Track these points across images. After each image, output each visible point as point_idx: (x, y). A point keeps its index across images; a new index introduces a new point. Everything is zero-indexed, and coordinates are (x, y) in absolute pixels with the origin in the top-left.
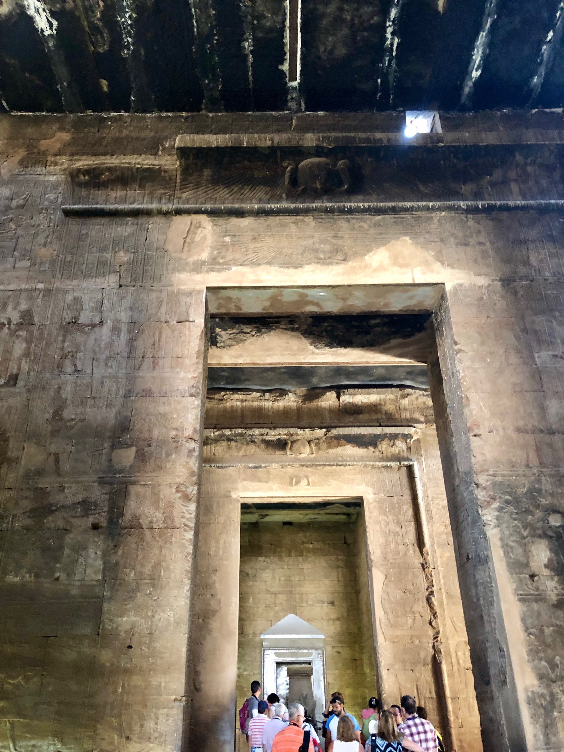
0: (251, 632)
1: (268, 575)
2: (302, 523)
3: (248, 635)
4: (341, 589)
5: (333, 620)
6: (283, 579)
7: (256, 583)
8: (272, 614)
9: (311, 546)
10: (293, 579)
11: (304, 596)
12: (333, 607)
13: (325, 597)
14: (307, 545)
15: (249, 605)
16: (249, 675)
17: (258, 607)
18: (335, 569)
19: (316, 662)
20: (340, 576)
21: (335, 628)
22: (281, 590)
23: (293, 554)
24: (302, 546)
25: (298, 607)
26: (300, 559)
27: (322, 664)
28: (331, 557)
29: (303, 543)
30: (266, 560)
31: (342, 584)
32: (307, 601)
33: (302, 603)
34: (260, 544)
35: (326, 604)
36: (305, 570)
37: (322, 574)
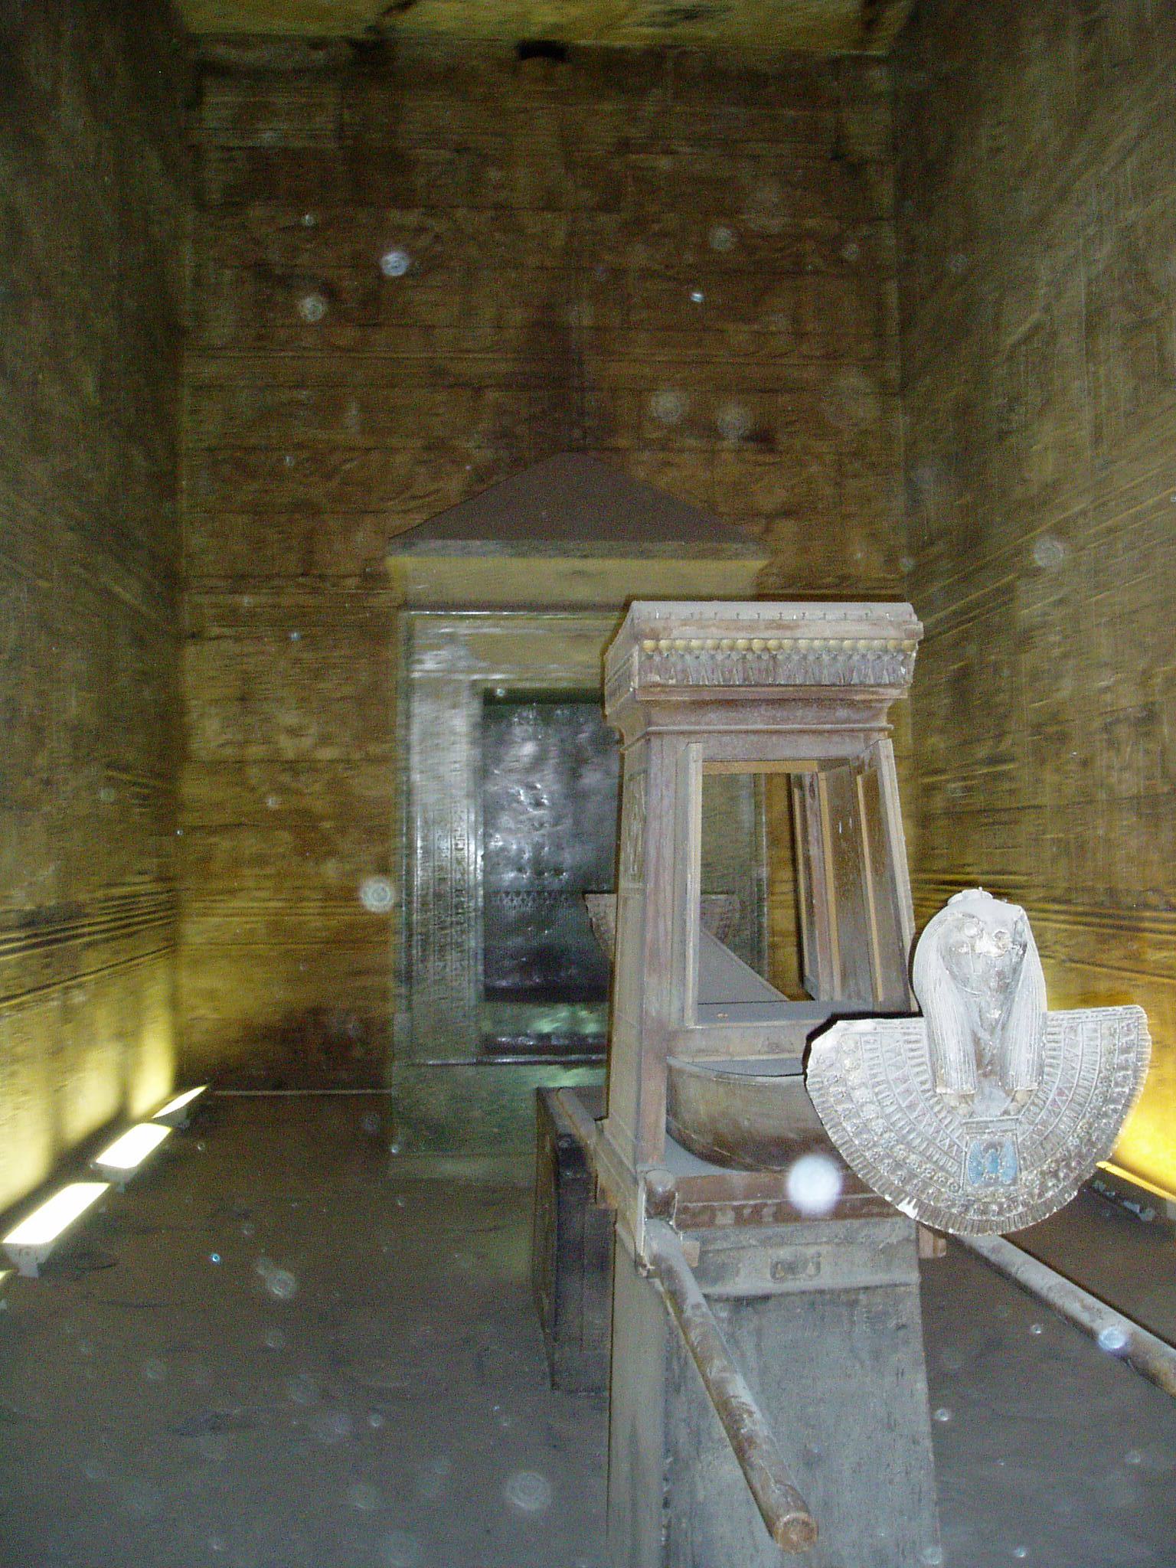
2: (623, 51)
6: (517, 316)
9: (664, 163)
12: (768, 458)
30: (430, 222)
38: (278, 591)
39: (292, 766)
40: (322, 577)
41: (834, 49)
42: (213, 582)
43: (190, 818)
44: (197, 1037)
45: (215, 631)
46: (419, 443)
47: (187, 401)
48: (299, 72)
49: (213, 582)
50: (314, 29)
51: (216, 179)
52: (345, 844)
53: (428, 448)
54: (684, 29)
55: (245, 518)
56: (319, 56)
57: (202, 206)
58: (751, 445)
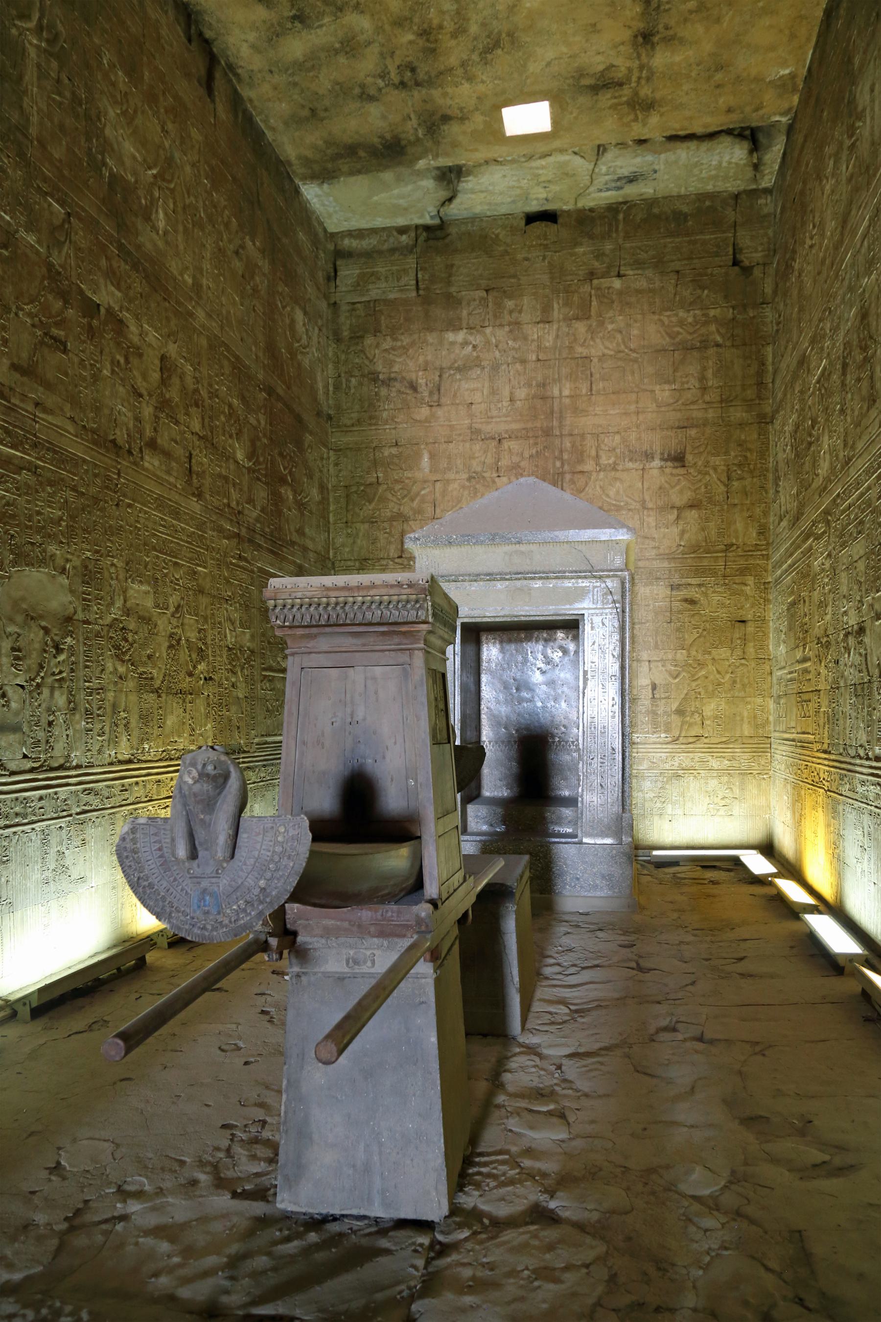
1: (472, 385)
2: (591, 210)
5: (679, 509)
7: (440, 412)
9: (617, 284)
10: (556, 392)
11: (590, 442)
12: (681, 471)
13: (655, 441)
14: (604, 282)
15: (419, 475)
17: (448, 481)
18: (695, 353)
19: (597, 620)
20: (709, 374)
21: (683, 532)
22: (514, 426)
24: (587, 288)
25: (568, 477)
26: (581, 327)
27: (616, 624)
28: (682, 314)
29: (592, 275)
30: (471, 338)
31: (713, 396)
33: (581, 461)
34: (453, 289)
35: (657, 463)
36: (595, 360)
37: (650, 370)
41: (733, 186)
42: (349, 563)
46: (466, 476)
47: (332, 459)
48: (393, 250)
49: (349, 563)
50: (401, 221)
51: (346, 323)
53: (469, 479)
54: (631, 191)
55: (366, 526)
56: (404, 238)
57: (338, 340)
58: (669, 464)
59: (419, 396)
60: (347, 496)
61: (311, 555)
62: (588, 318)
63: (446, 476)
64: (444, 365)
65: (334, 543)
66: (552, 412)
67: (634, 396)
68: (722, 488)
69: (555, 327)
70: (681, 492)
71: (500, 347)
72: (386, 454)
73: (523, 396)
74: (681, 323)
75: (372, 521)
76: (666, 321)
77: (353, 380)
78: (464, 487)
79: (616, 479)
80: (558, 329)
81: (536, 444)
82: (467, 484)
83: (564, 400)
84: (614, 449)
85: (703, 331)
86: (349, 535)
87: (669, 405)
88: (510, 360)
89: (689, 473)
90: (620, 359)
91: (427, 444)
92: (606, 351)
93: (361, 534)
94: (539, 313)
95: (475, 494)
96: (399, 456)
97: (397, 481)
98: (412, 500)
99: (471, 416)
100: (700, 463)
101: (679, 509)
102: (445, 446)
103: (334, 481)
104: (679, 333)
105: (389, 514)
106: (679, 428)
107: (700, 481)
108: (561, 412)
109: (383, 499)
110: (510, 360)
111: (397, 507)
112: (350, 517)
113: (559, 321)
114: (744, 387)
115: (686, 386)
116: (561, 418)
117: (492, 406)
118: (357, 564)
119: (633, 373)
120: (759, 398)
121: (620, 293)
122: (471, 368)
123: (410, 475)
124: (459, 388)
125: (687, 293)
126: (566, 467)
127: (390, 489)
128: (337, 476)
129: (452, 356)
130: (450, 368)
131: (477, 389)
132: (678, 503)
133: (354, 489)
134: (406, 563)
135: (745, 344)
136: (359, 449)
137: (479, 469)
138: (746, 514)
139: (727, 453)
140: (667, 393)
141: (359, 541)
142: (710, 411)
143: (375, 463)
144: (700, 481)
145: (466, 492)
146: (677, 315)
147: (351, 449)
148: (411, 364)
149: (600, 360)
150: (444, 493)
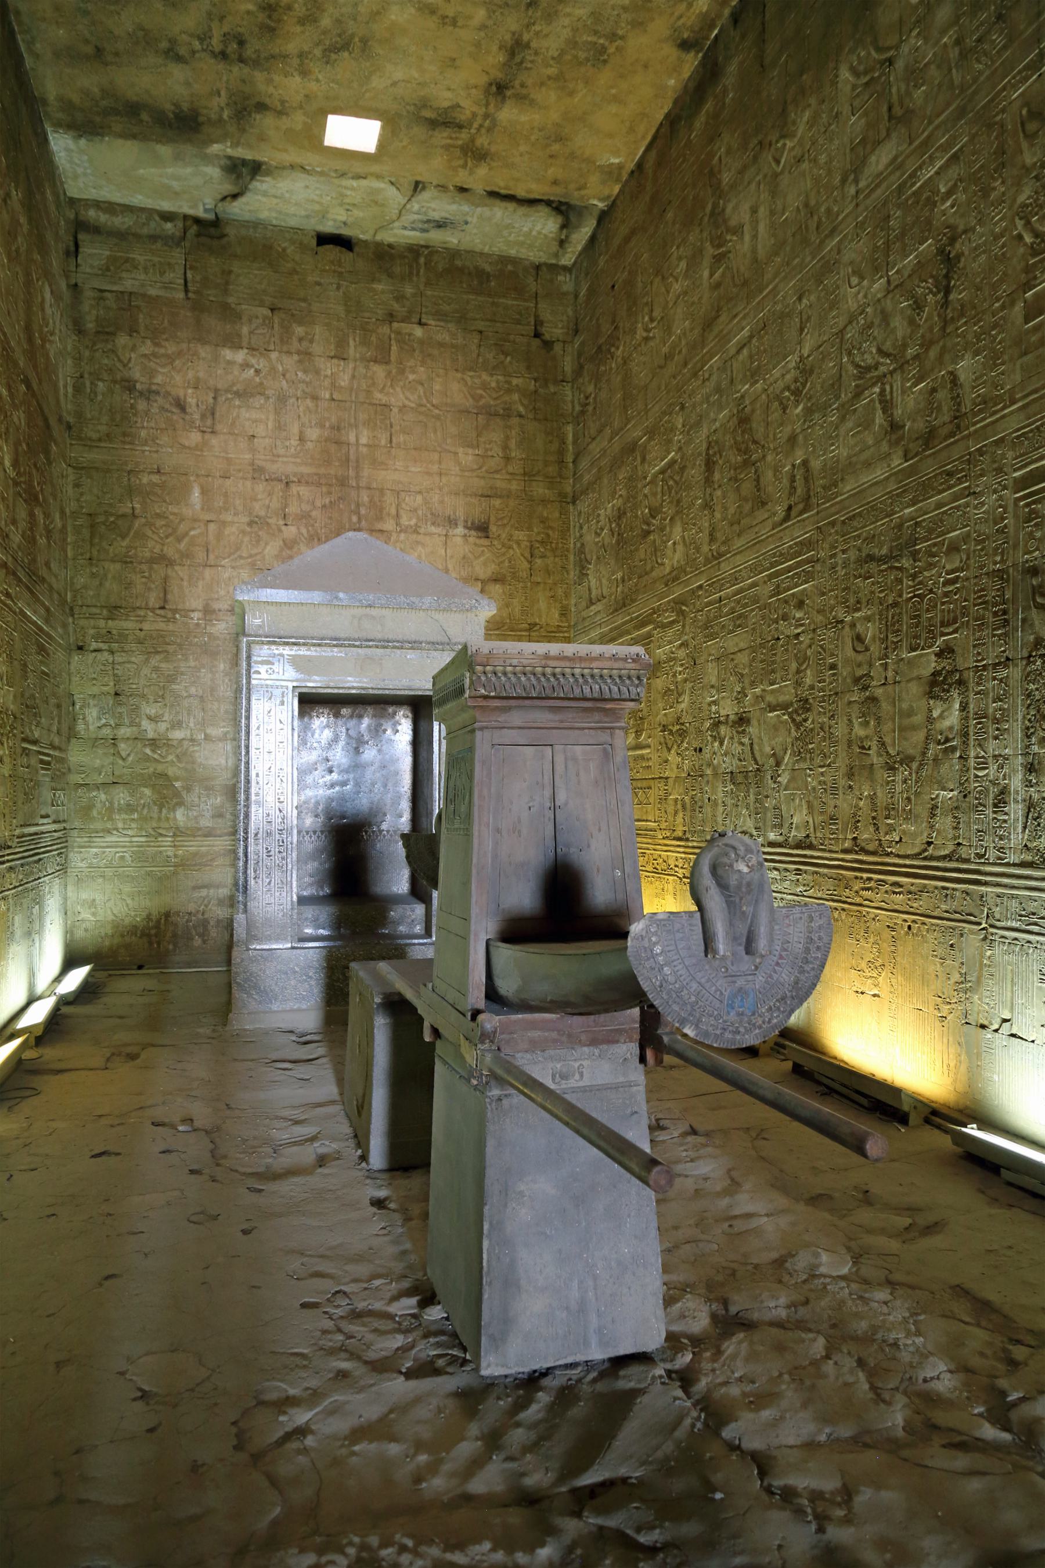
0: (196, 603)
1: (254, 415)
3: (186, 613)
4: (514, 486)
5: (484, 582)
6: (313, 434)
7: (214, 441)
8: (271, 549)
10: (352, 438)
11: (389, 499)
12: (486, 542)
13: (459, 507)
15: (187, 512)
16: (192, 740)
17: (224, 524)
20: (513, 444)
22: (306, 470)
23: (352, 351)
26: (379, 371)
28: (485, 376)
31: (515, 467)
32: (398, 515)
33: (380, 518)
35: (460, 530)
36: (395, 410)
37: (453, 430)
38: (142, 619)
39: (154, 743)
40: (175, 611)
43: (75, 778)
44: (80, 934)
45: (94, 645)
46: (246, 519)
52: (191, 798)
53: (250, 524)
55: (118, 566)
59: (187, 417)
60: (92, 526)
61: (56, 596)
62: (388, 362)
63: (223, 517)
64: (219, 386)
65: (72, 583)
66: (348, 460)
67: (436, 456)
68: (526, 565)
69: (351, 365)
70: (485, 564)
71: (288, 376)
72: (145, 480)
73: (314, 437)
74: (485, 386)
75: (126, 561)
76: (468, 379)
77: (100, 384)
78: (243, 532)
79: (418, 543)
80: (355, 368)
81: (330, 493)
82: (248, 529)
83: (361, 448)
84: (416, 510)
85: (506, 398)
86: (93, 575)
87: (473, 470)
88: (299, 393)
89: (492, 545)
90: (421, 413)
91: (197, 476)
92: (407, 402)
93: (110, 576)
94: (332, 347)
95: (258, 541)
96: (162, 486)
97: (159, 516)
98: (179, 540)
99: (253, 450)
100: (504, 536)
101: (484, 582)
102: (221, 481)
103: (74, 505)
104: (481, 396)
105: (148, 555)
106: (482, 496)
107: (504, 554)
108: (357, 461)
109: (141, 536)
110: (299, 393)
111: (158, 546)
112: (95, 553)
113: (355, 360)
114: (546, 464)
115: (490, 453)
116: (358, 468)
117: (279, 443)
118: (105, 612)
119: (435, 431)
120: (561, 476)
121: (421, 342)
122: (252, 395)
123: (176, 511)
124: (238, 416)
125: (490, 356)
126: (363, 523)
127: (149, 524)
128: (78, 500)
129: (230, 377)
130: (227, 391)
131: (261, 421)
132: (482, 576)
133: (101, 519)
134: (170, 615)
135: (546, 419)
136: (108, 471)
137: (262, 513)
138: (549, 594)
139: (530, 528)
140: (470, 458)
141: (107, 584)
142: (514, 482)
143: (130, 492)
144: (504, 554)
145: (246, 539)
146: (480, 377)
147: (97, 469)
148: (178, 379)
149: (400, 411)
150: (219, 537)
